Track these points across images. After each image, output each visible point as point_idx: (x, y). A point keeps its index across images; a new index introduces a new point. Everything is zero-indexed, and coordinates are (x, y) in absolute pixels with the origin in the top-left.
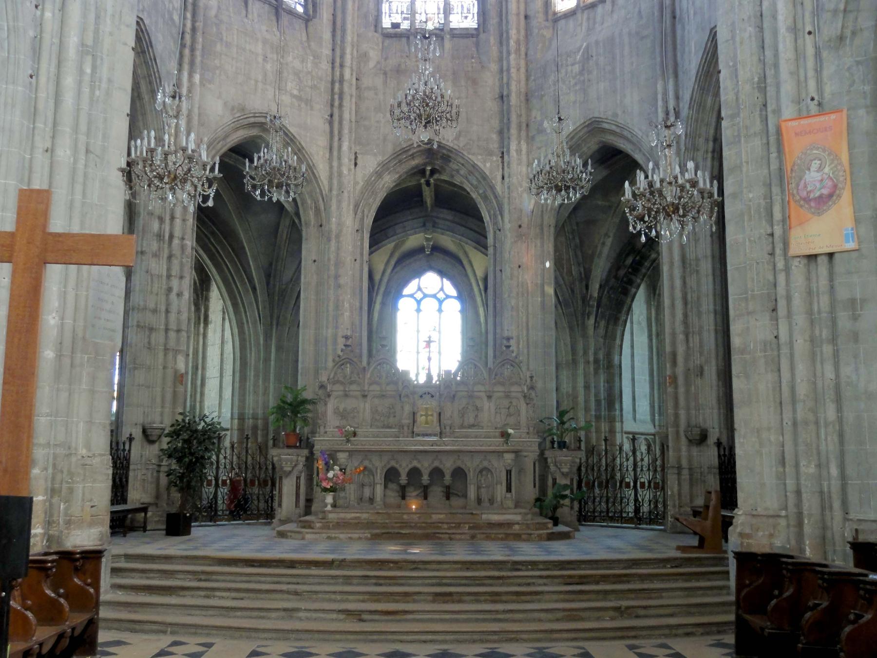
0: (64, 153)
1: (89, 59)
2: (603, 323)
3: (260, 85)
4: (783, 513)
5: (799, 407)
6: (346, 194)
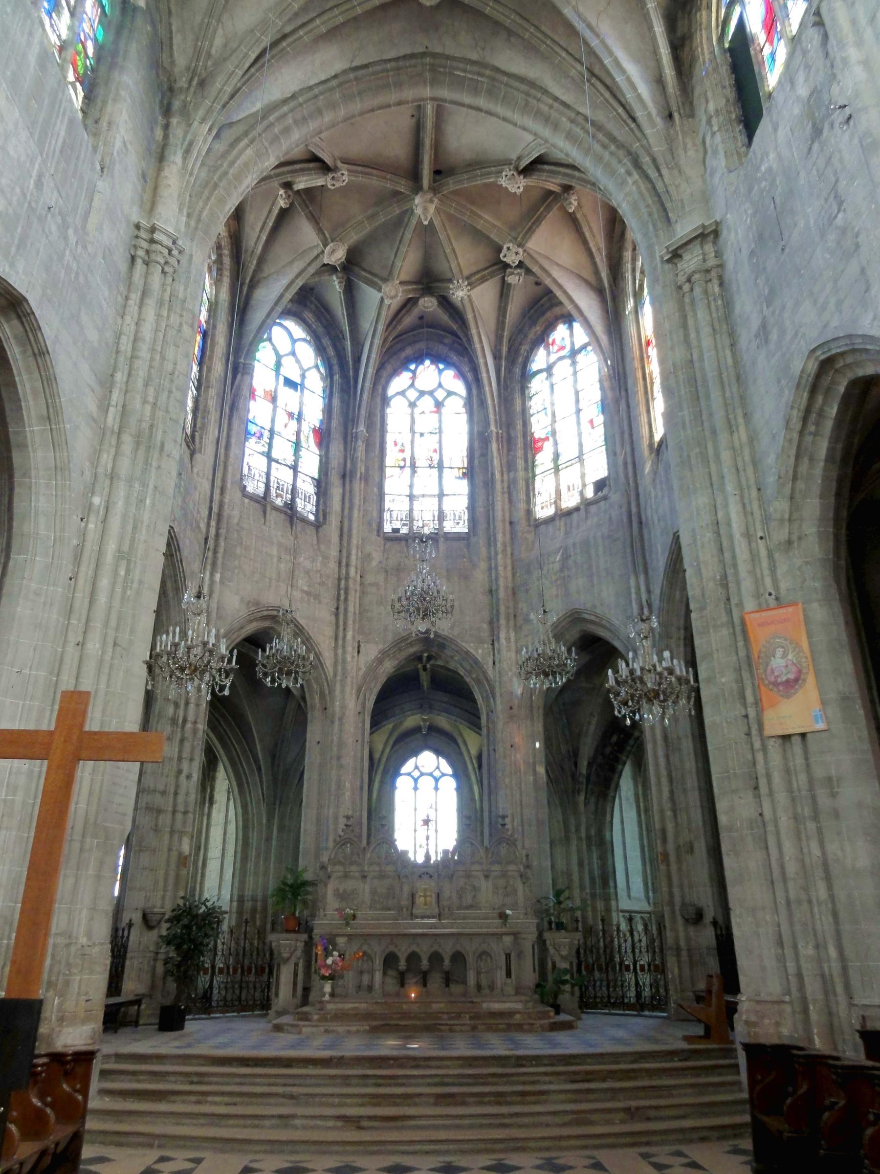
0: (93, 646)
1: (124, 563)
2: (593, 800)
3: (274, 583)
4: (787, 999)
5: (791, 885)
6: (349, 679)
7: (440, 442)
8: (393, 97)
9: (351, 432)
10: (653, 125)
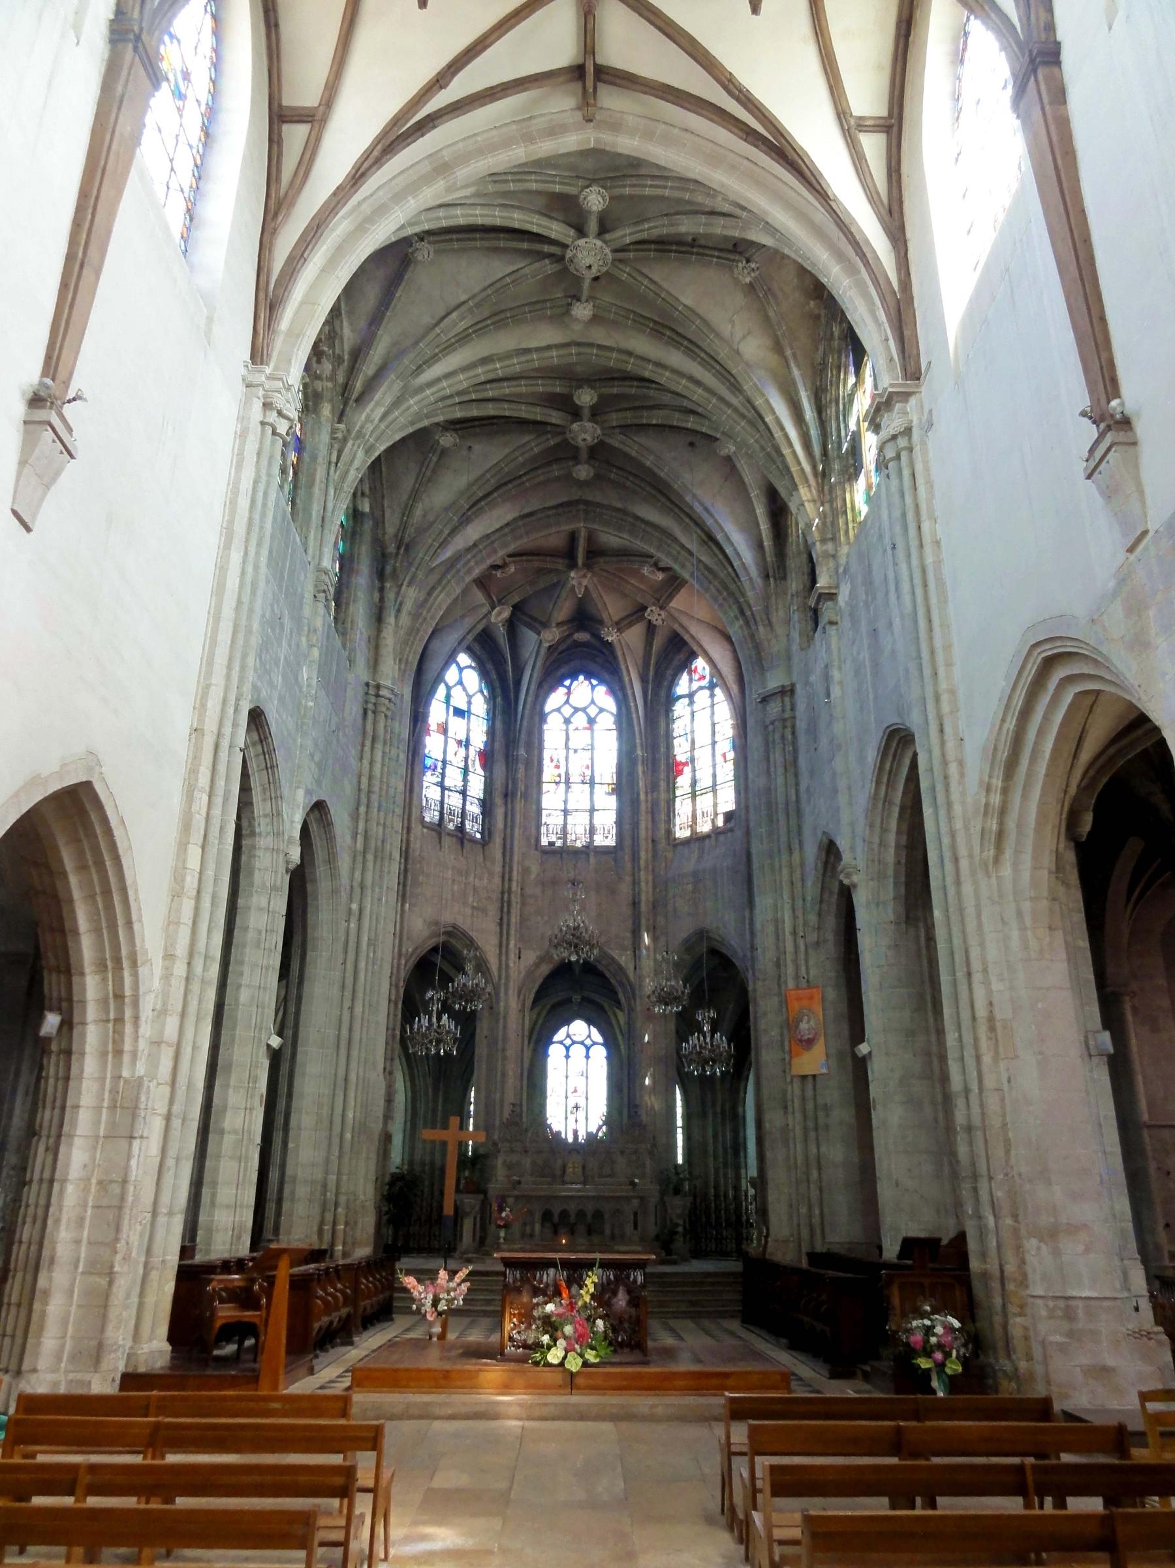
0: (358, 1010)
1: (372, 948)
7: (592, 759)
8: (554, 530)
9: (512, 751)
10: (753, 588)
